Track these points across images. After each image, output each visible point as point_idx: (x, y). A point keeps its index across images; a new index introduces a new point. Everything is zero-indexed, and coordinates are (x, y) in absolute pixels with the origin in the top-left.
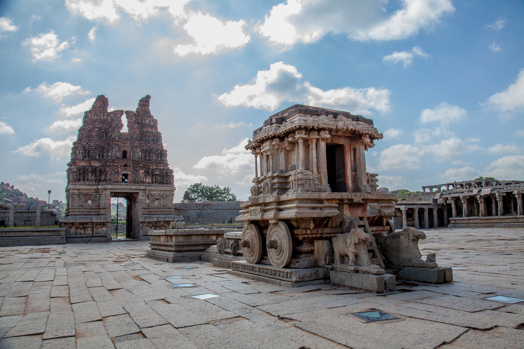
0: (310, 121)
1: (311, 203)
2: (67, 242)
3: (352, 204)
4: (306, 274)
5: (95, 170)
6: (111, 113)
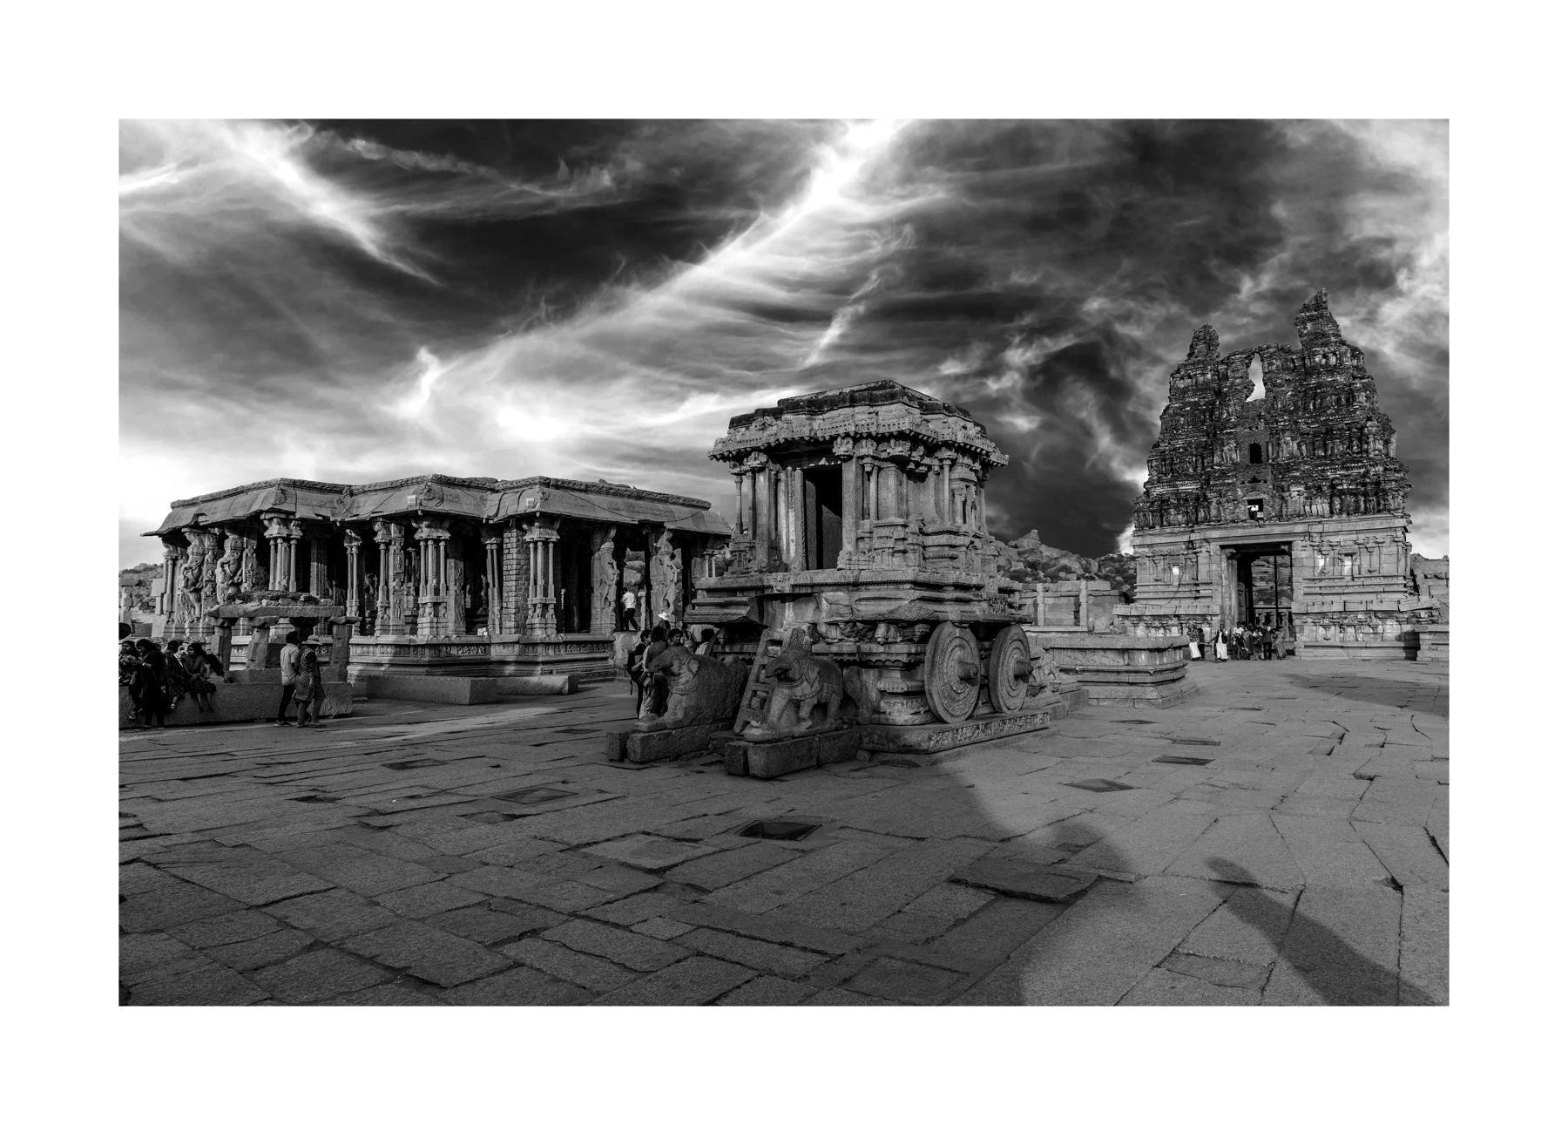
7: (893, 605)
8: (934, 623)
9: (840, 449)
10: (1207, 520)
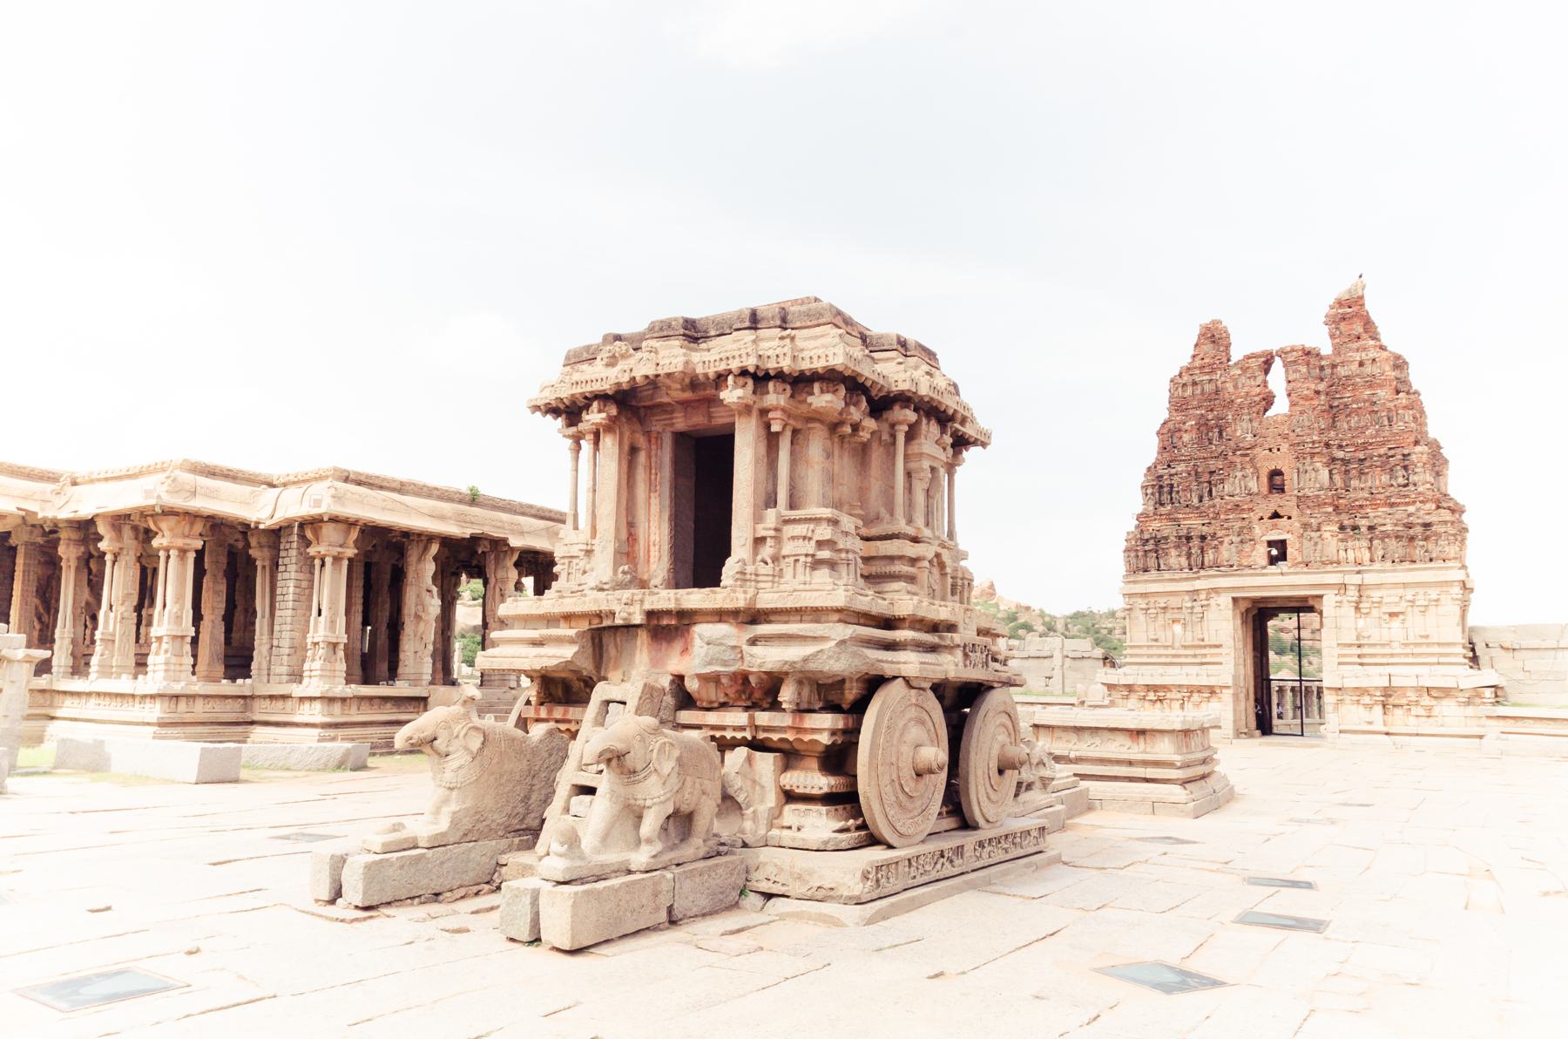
7: (809, 649)
8: (874, 683)
9: (732, 394)
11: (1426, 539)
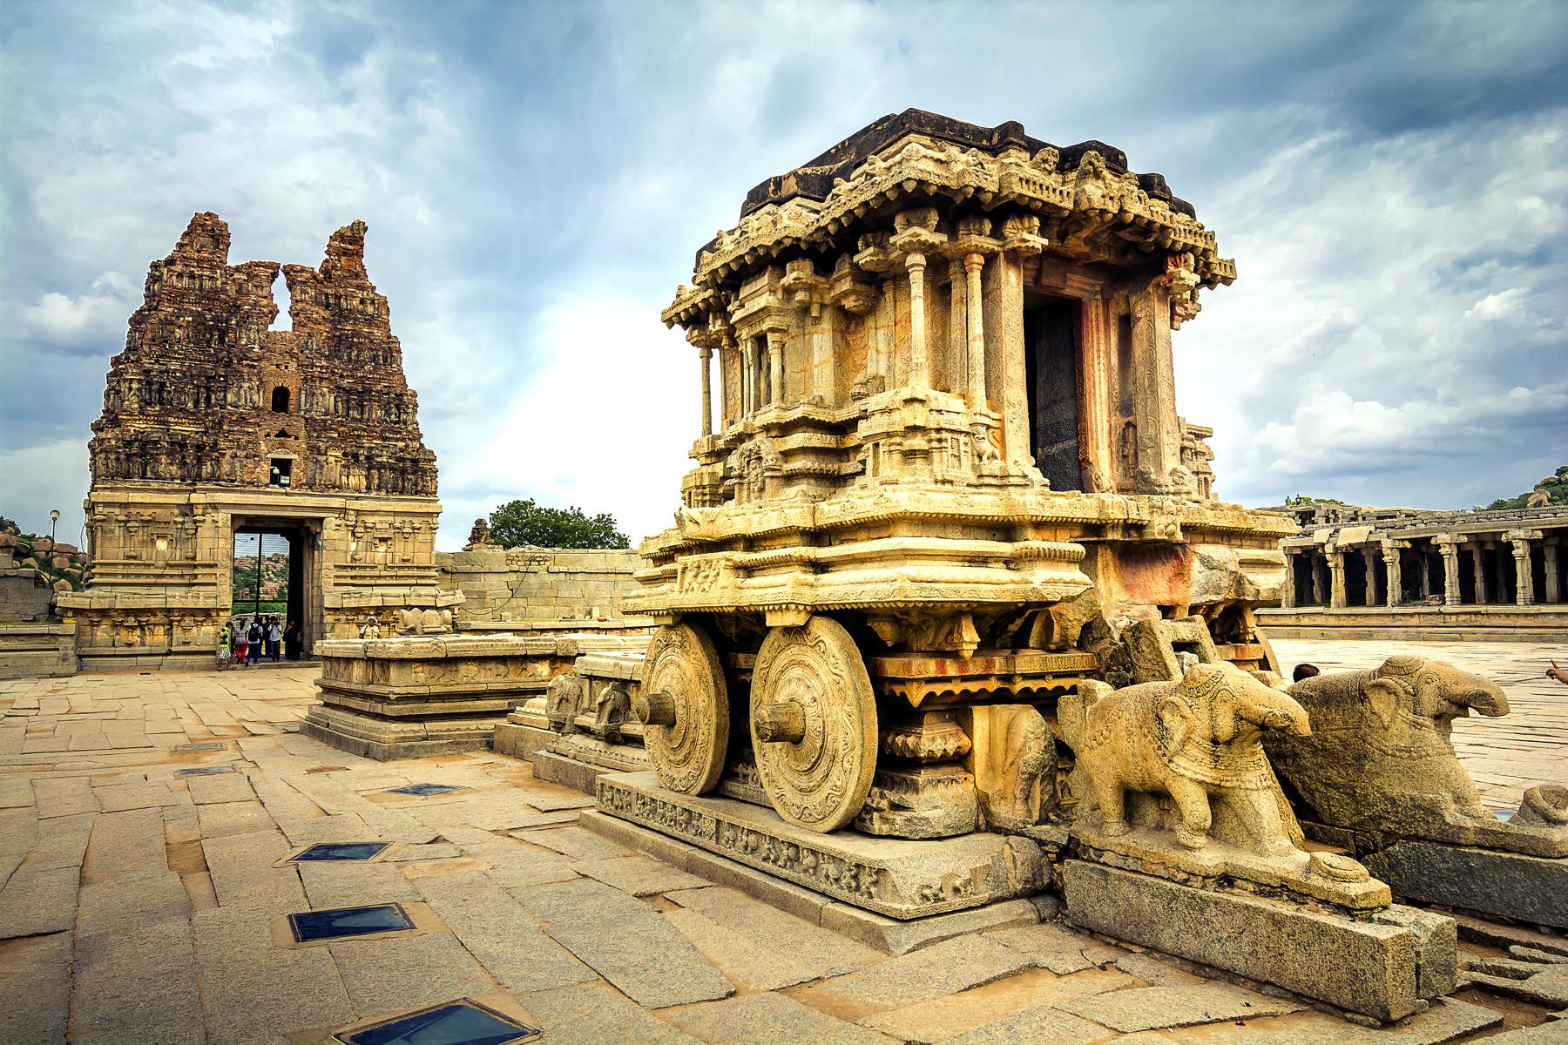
0: (963, 168)
1: (965, 536)
2: (81, 670)
3: (1137, 550)
4: (952, 876)
5: (183, 446)
6: (238, 269)
10: (213, 478)
11: (414, 473)
